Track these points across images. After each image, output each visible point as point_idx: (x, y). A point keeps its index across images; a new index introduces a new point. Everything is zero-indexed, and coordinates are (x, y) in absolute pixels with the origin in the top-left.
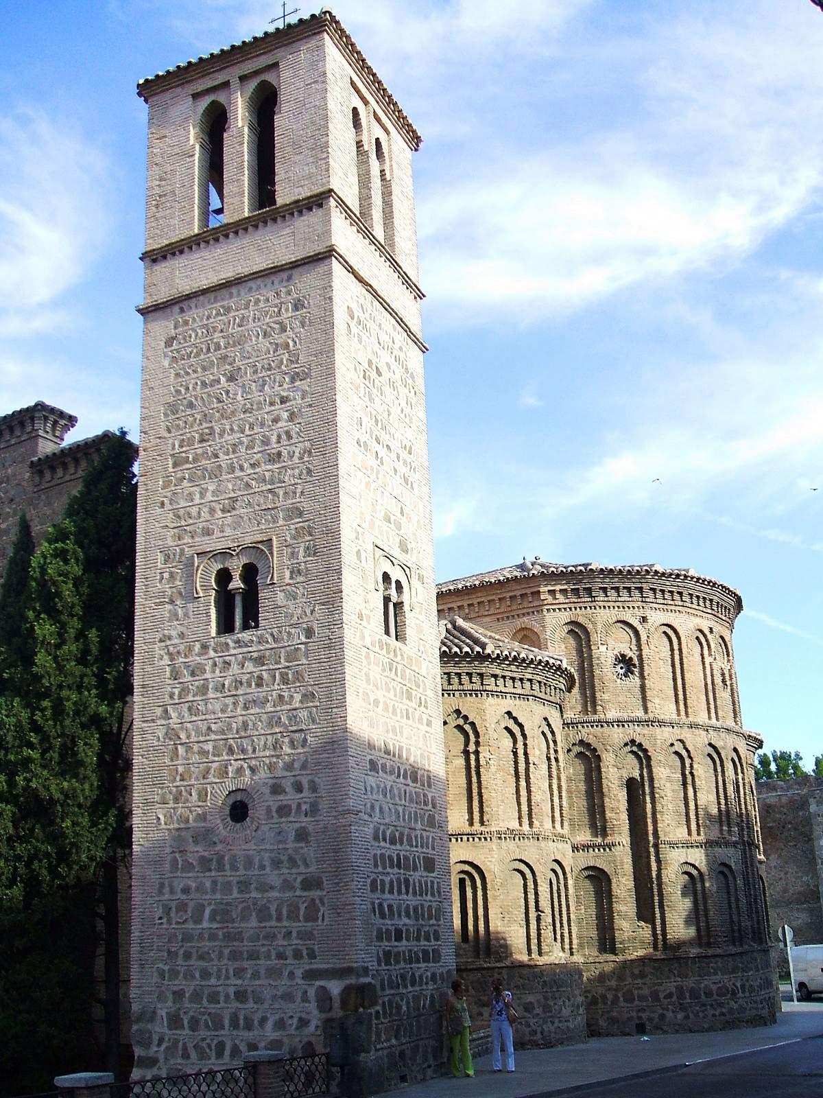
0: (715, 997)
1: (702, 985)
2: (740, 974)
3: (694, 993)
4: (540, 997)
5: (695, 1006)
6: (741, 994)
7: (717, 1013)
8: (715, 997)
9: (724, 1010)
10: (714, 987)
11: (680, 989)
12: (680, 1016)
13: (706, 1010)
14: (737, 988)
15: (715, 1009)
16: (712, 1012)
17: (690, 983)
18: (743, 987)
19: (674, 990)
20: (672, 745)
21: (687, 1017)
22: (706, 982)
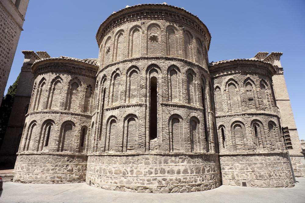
0: (113, 174)
1: (108, 168)
2: (131, 165)
3: (104, 170)
4: (26, 165)
5: (104, 177)
6: (129, 175)
7: (113, 182)
8: (113, 174)
9: (116, 181)
10: (113, 170)
11: (101, 168)
12: (99, 180)
13: (108, 179)
14: (127, 171)
15: (112, 179)
16: (110, 181)
17: (103, 167)
18: (132, 171)
19: (99, 169)
20: (114, 72)
21: (101, 181)
22: (110, 167)
